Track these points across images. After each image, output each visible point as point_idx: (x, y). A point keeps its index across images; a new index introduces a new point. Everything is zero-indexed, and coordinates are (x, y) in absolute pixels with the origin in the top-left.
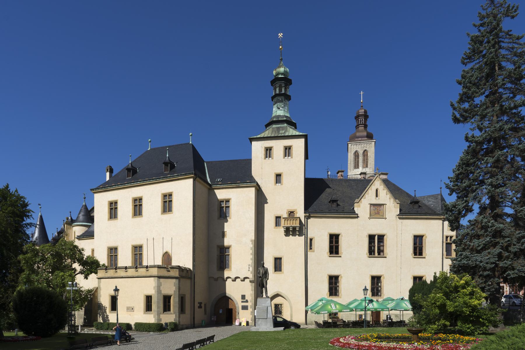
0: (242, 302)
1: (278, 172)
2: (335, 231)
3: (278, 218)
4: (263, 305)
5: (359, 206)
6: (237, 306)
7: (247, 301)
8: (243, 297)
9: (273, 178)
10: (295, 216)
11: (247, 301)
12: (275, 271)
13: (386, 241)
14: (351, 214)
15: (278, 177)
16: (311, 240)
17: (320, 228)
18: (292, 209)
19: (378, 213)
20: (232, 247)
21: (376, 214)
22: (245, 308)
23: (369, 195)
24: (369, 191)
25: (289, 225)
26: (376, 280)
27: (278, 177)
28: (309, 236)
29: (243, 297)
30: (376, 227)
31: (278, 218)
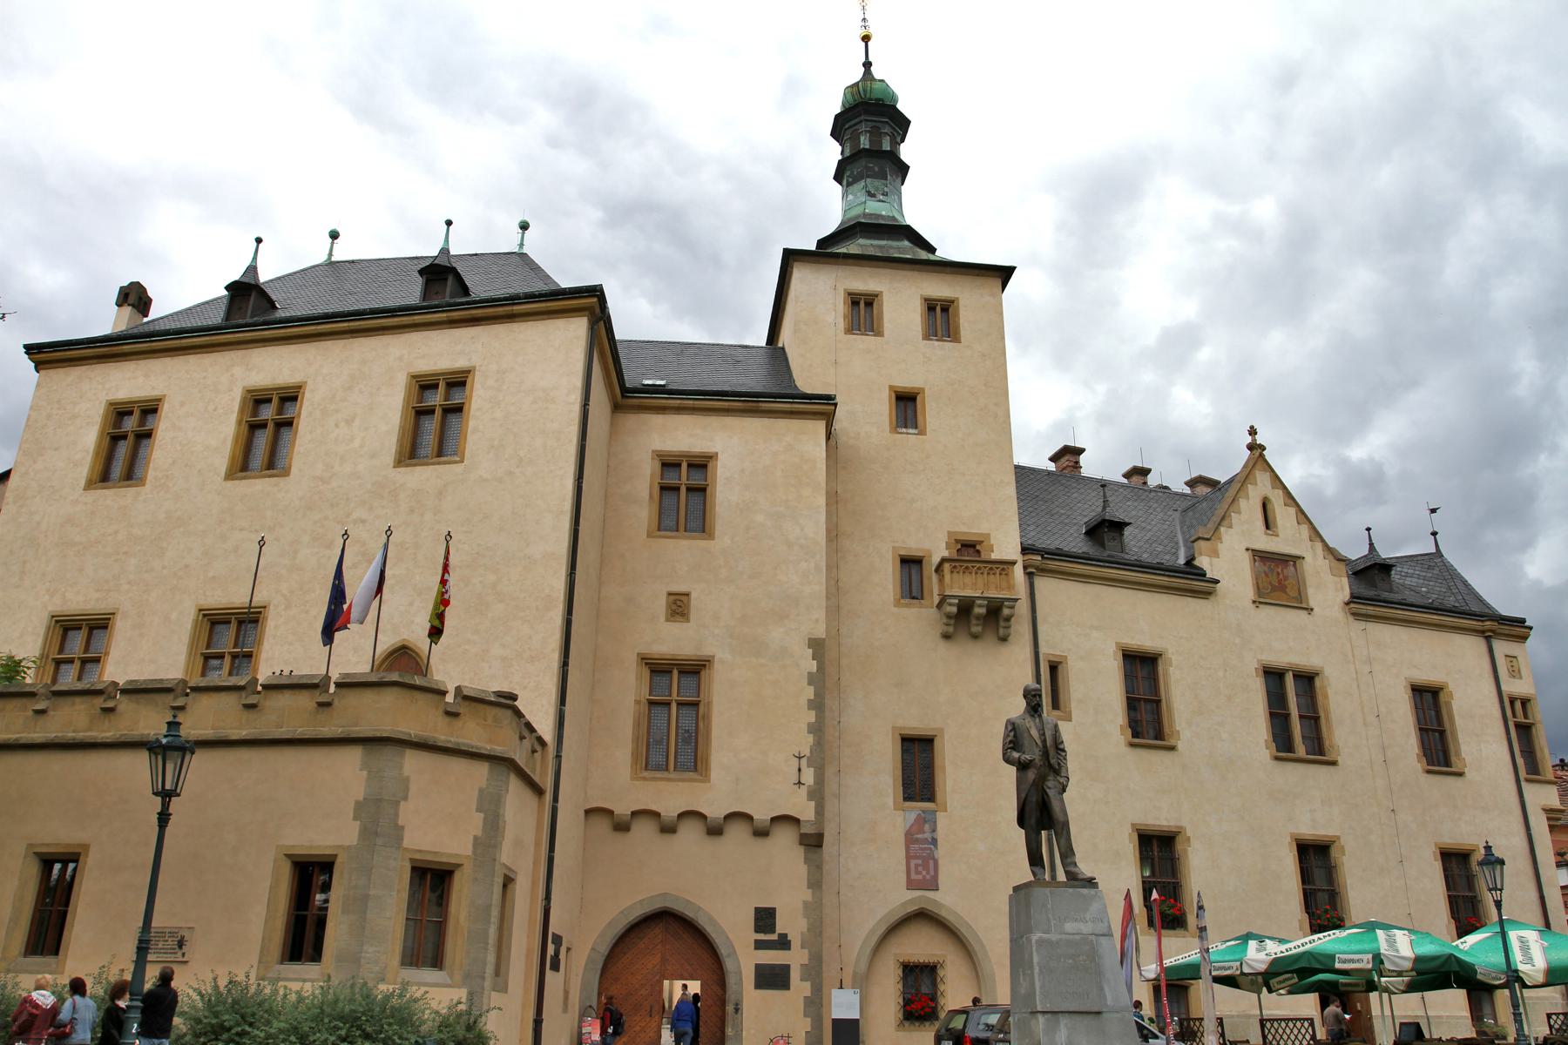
0: (759, 945)
1: (906, 382)
2: (1144, 641)
3: (911, 563)
4: (1070, 927)
5: (1215, 553)
6: (729, 965)
7: (783, 943)
8: (765, 918)
9: (883, 407)
10: (984, 557)
11: (783, 943)
12: (906, 799)
13: (1326, 696)
14: (1190, 580)
15: (906, 404)
16: (1054, 668)
17: (1088, 625)
18: (971, 530)
19: (1281, 587)
20: (717, 665)
21: (1274, 589)
22: (771, 978)
23: (1244, 516)
24: (1243, 503)
25: (968, 593)
26: (1315, 858)
27: (906, 404)
28: (1044, 649)
29: (765, 918)
30: (1288, 639)
31: (911, 563)
